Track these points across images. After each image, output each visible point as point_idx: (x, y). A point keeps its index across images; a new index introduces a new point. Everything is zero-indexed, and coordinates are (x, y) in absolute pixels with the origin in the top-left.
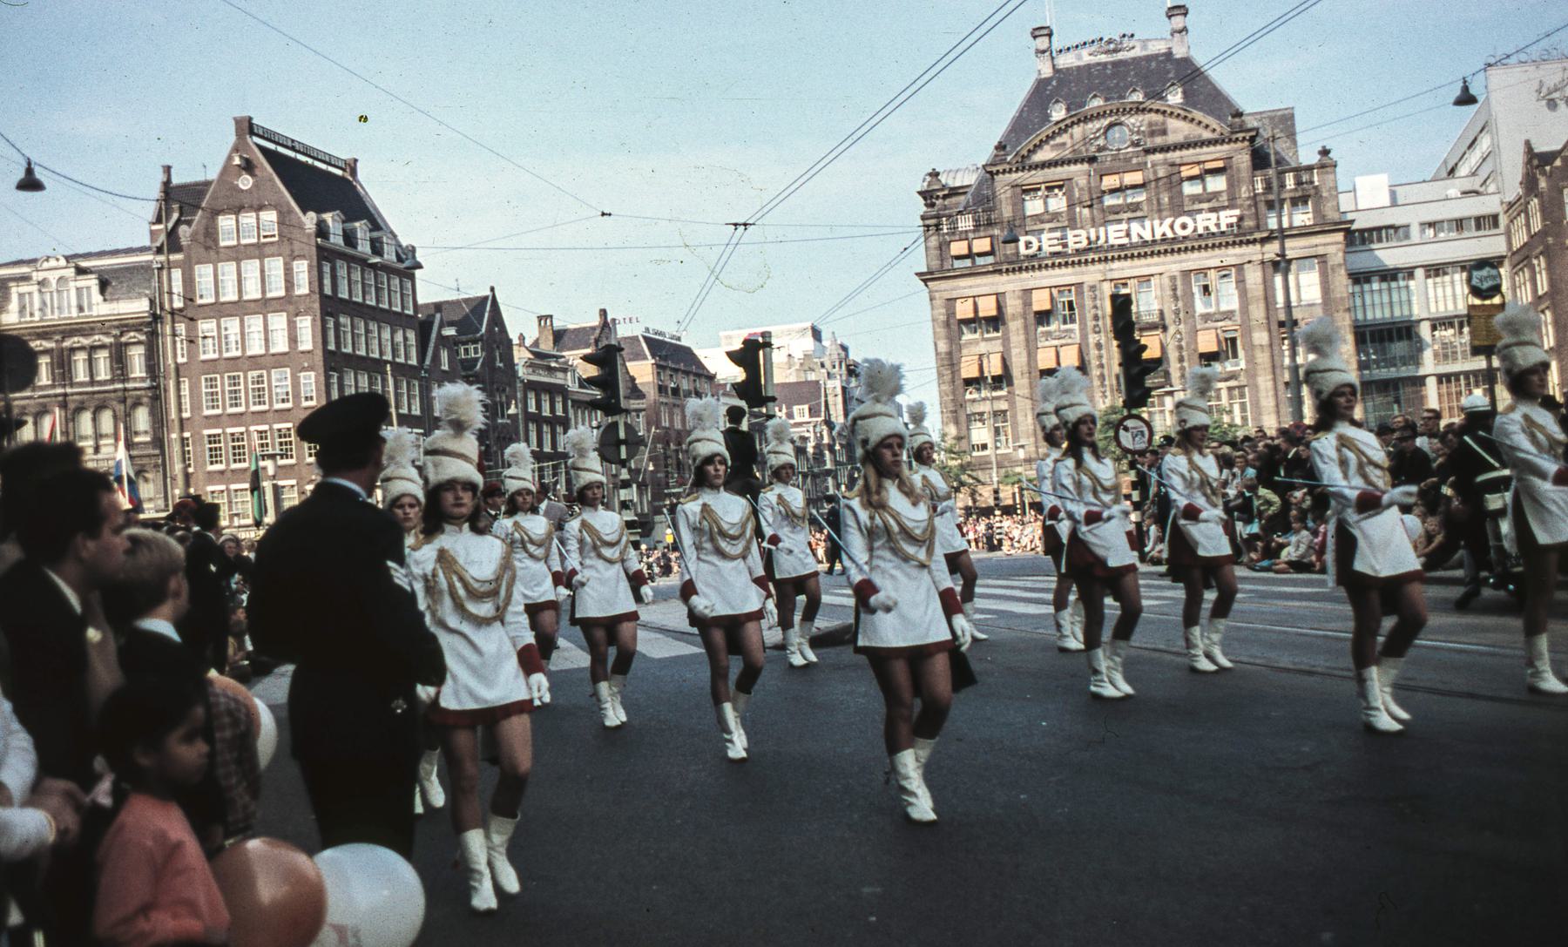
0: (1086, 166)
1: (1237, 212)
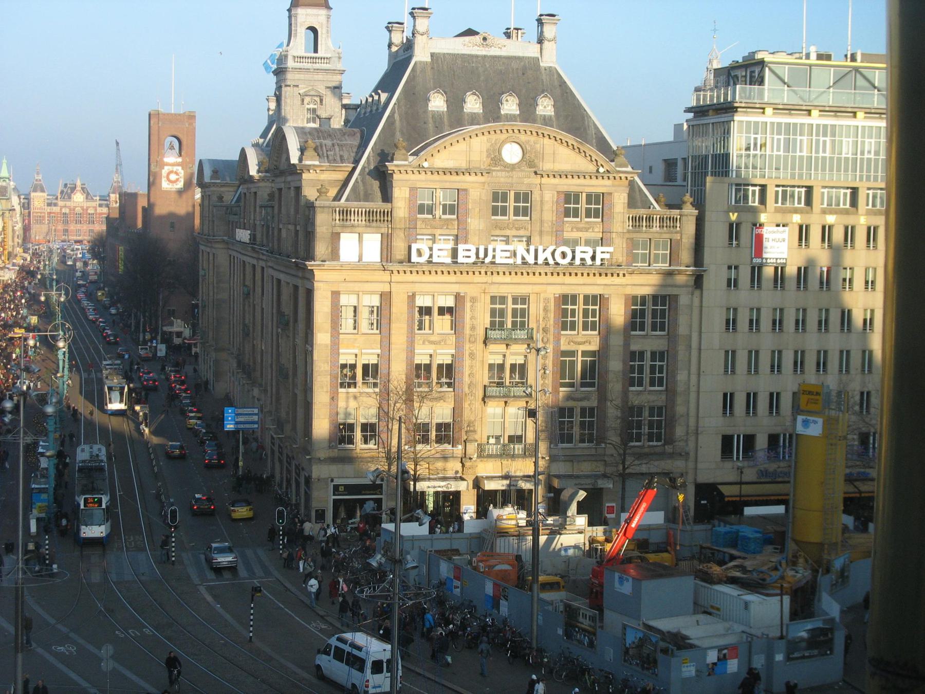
1: (611, 249)
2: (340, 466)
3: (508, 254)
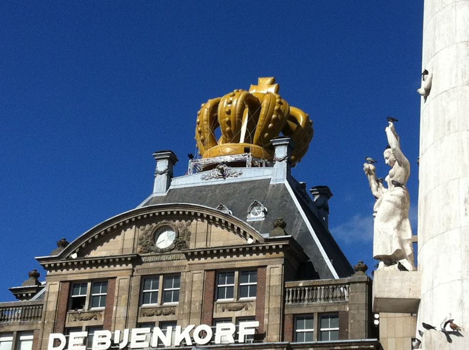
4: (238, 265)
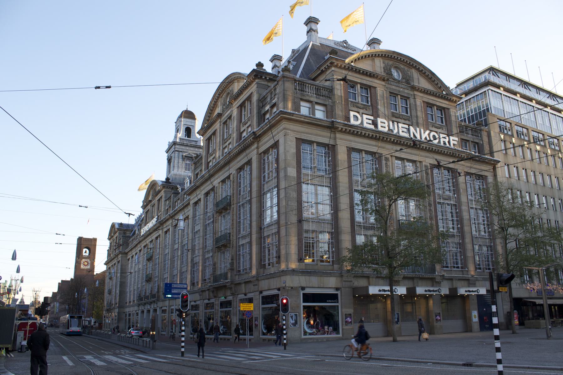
0: (383, 83)
1: (457, 139)
2: (307, 278)
3: (405, 130)
4: (438, 104)
